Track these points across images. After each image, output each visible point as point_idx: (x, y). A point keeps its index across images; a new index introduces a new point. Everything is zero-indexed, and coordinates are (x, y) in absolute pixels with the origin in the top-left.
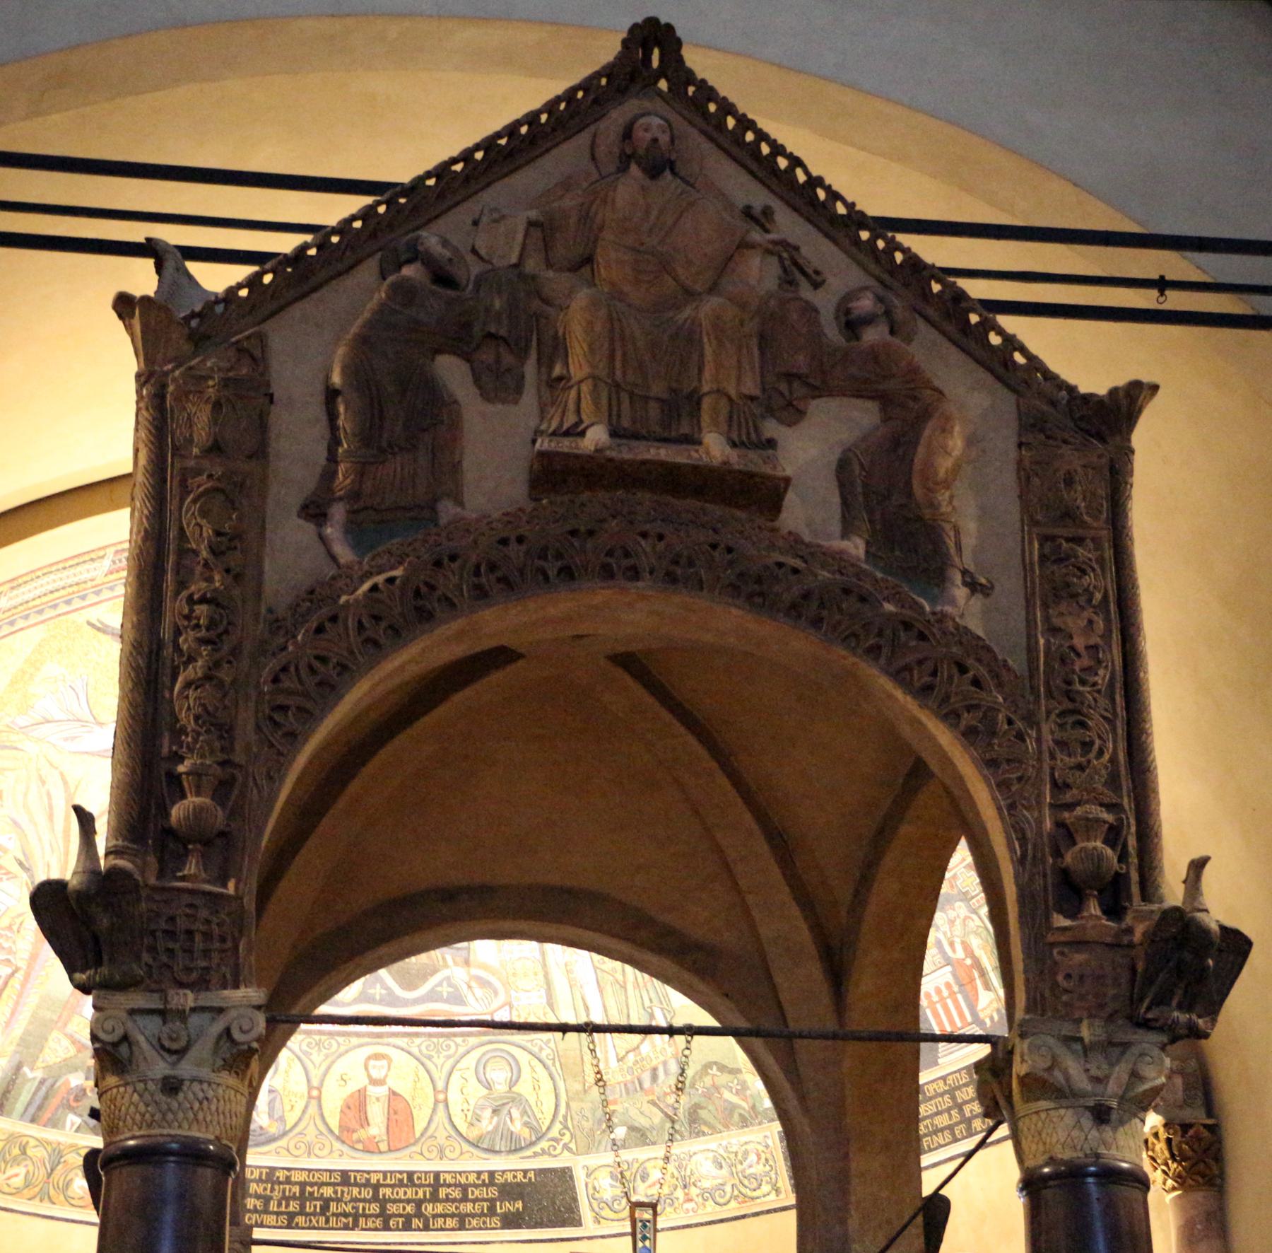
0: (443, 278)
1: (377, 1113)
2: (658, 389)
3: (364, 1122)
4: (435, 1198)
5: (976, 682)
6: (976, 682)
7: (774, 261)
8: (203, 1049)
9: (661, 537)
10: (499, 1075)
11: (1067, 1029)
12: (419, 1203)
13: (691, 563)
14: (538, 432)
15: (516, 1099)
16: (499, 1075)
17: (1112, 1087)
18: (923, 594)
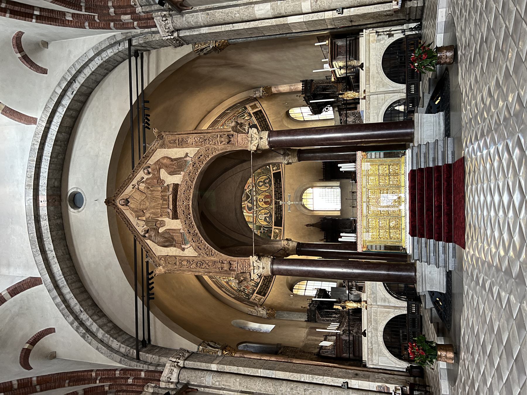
0: (147, 232)
1: (266, 200)
2: (161, 202)
3: (268, 201)
4: (278, 191)
5: (201, 156)
6: (201, 156)
7: (141, 184)
8: (258, 264)
9: (183, 201)
10: (261, 184)
11: (250, 143)
12: (278, 193)
13: (186, 197)
14: (169, 218)
15: (264, 181)
16: (261, 184)
17: (257, 137)
18: (189, 163)
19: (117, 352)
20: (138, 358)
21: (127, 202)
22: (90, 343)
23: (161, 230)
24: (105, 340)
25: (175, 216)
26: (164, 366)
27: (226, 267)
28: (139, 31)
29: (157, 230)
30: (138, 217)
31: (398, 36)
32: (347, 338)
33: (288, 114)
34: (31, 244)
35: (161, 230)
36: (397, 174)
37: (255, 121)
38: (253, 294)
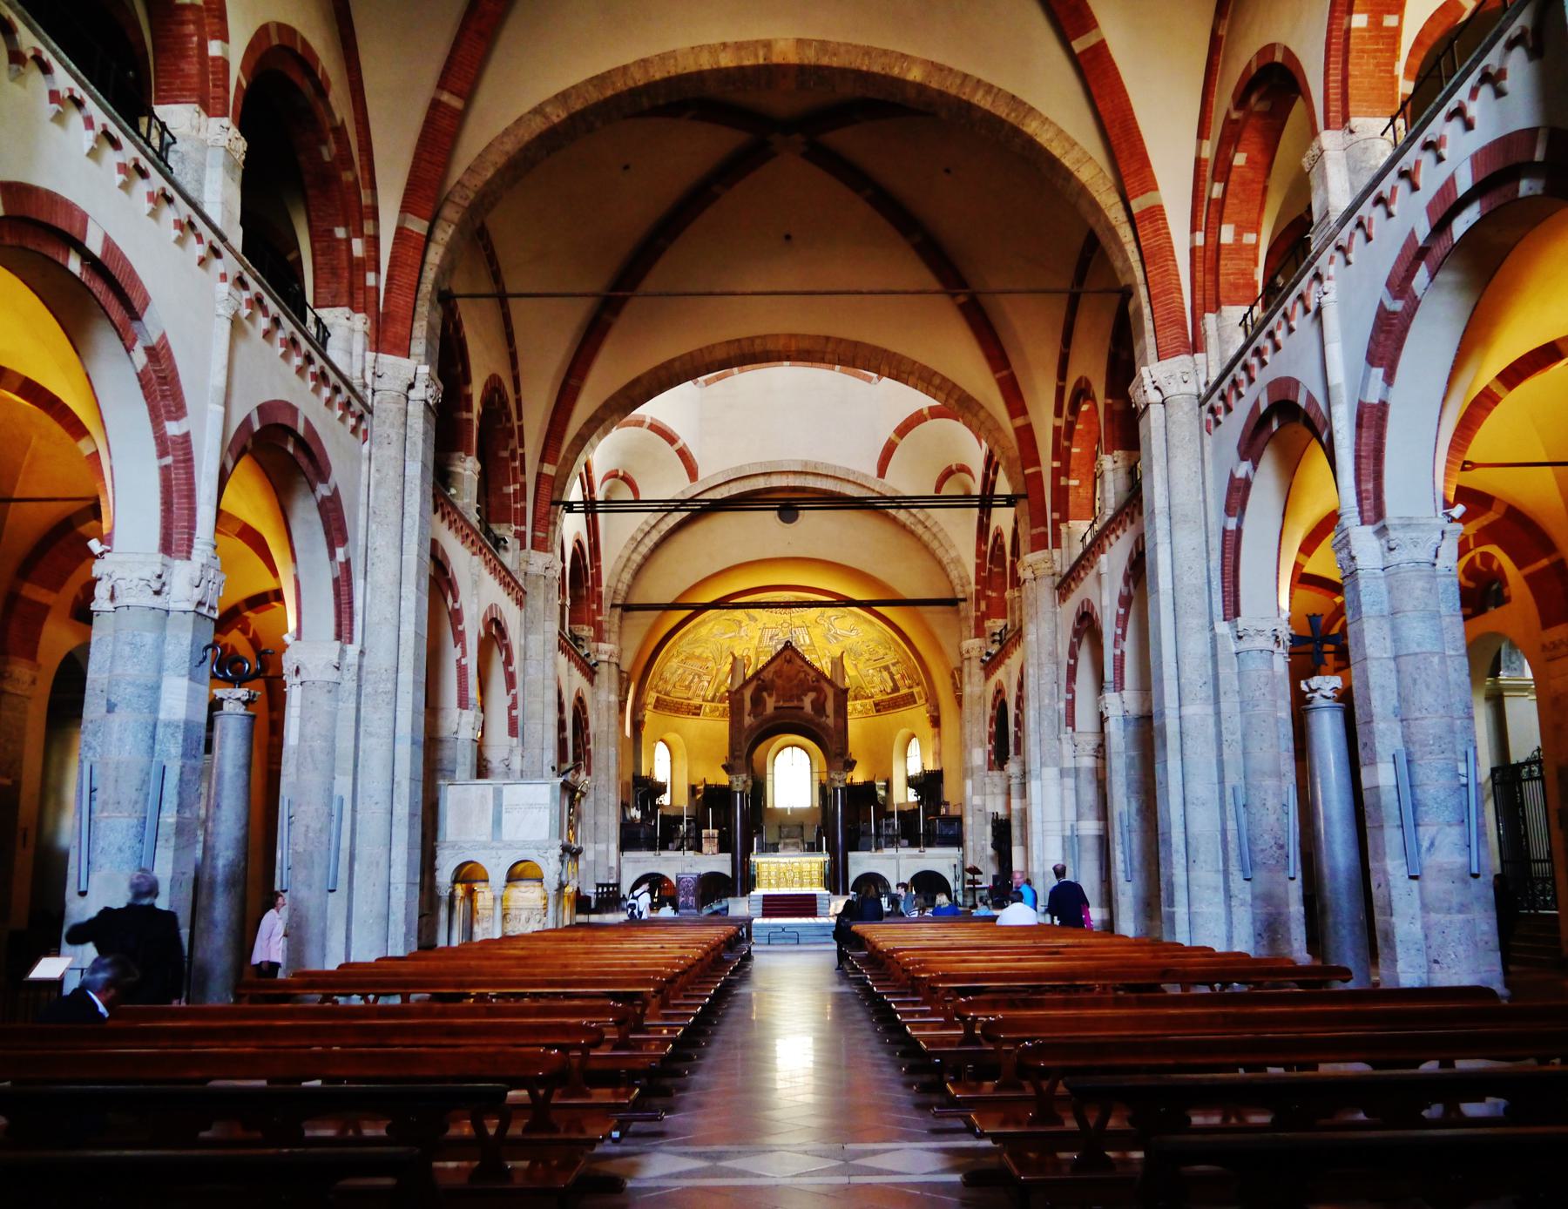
19: (619, 581)
20: (613, 606)
21: (789, 662)
22: (625, 546)
23: (765, 694)
24: (630, 564)
25: (776, 708)
26: (610, 643)
27: (737, 753)
28: (974, 614)
29: (765, 689)
30: (775, 672)
31: (952, 888)
32: (642, 836)
33: (913, 736)
34: (737, 468)
35: (765, 694)
36: (811, 884)
37: (904, 691)
38: (658, 692)
